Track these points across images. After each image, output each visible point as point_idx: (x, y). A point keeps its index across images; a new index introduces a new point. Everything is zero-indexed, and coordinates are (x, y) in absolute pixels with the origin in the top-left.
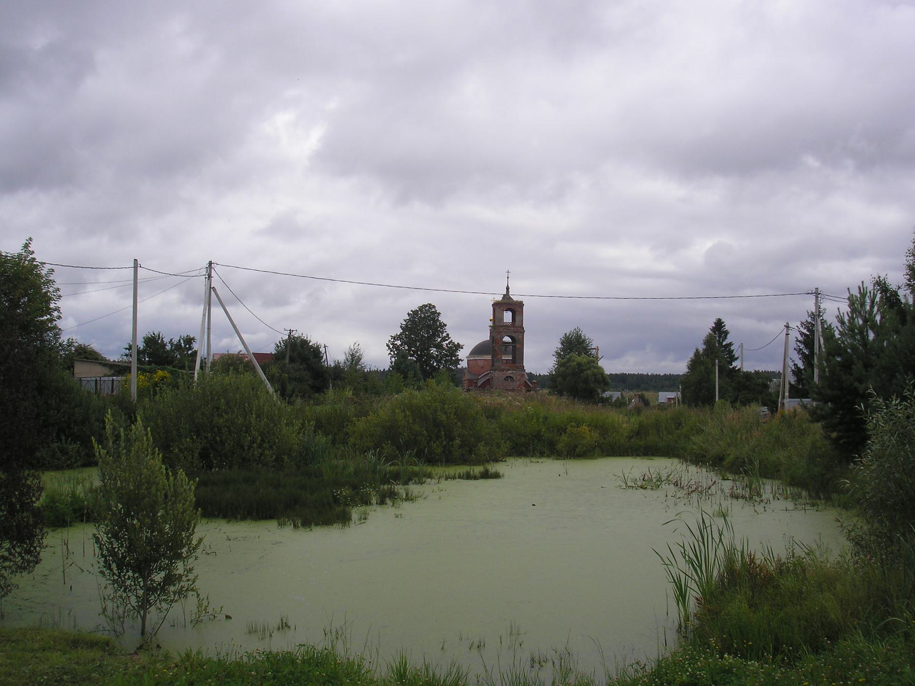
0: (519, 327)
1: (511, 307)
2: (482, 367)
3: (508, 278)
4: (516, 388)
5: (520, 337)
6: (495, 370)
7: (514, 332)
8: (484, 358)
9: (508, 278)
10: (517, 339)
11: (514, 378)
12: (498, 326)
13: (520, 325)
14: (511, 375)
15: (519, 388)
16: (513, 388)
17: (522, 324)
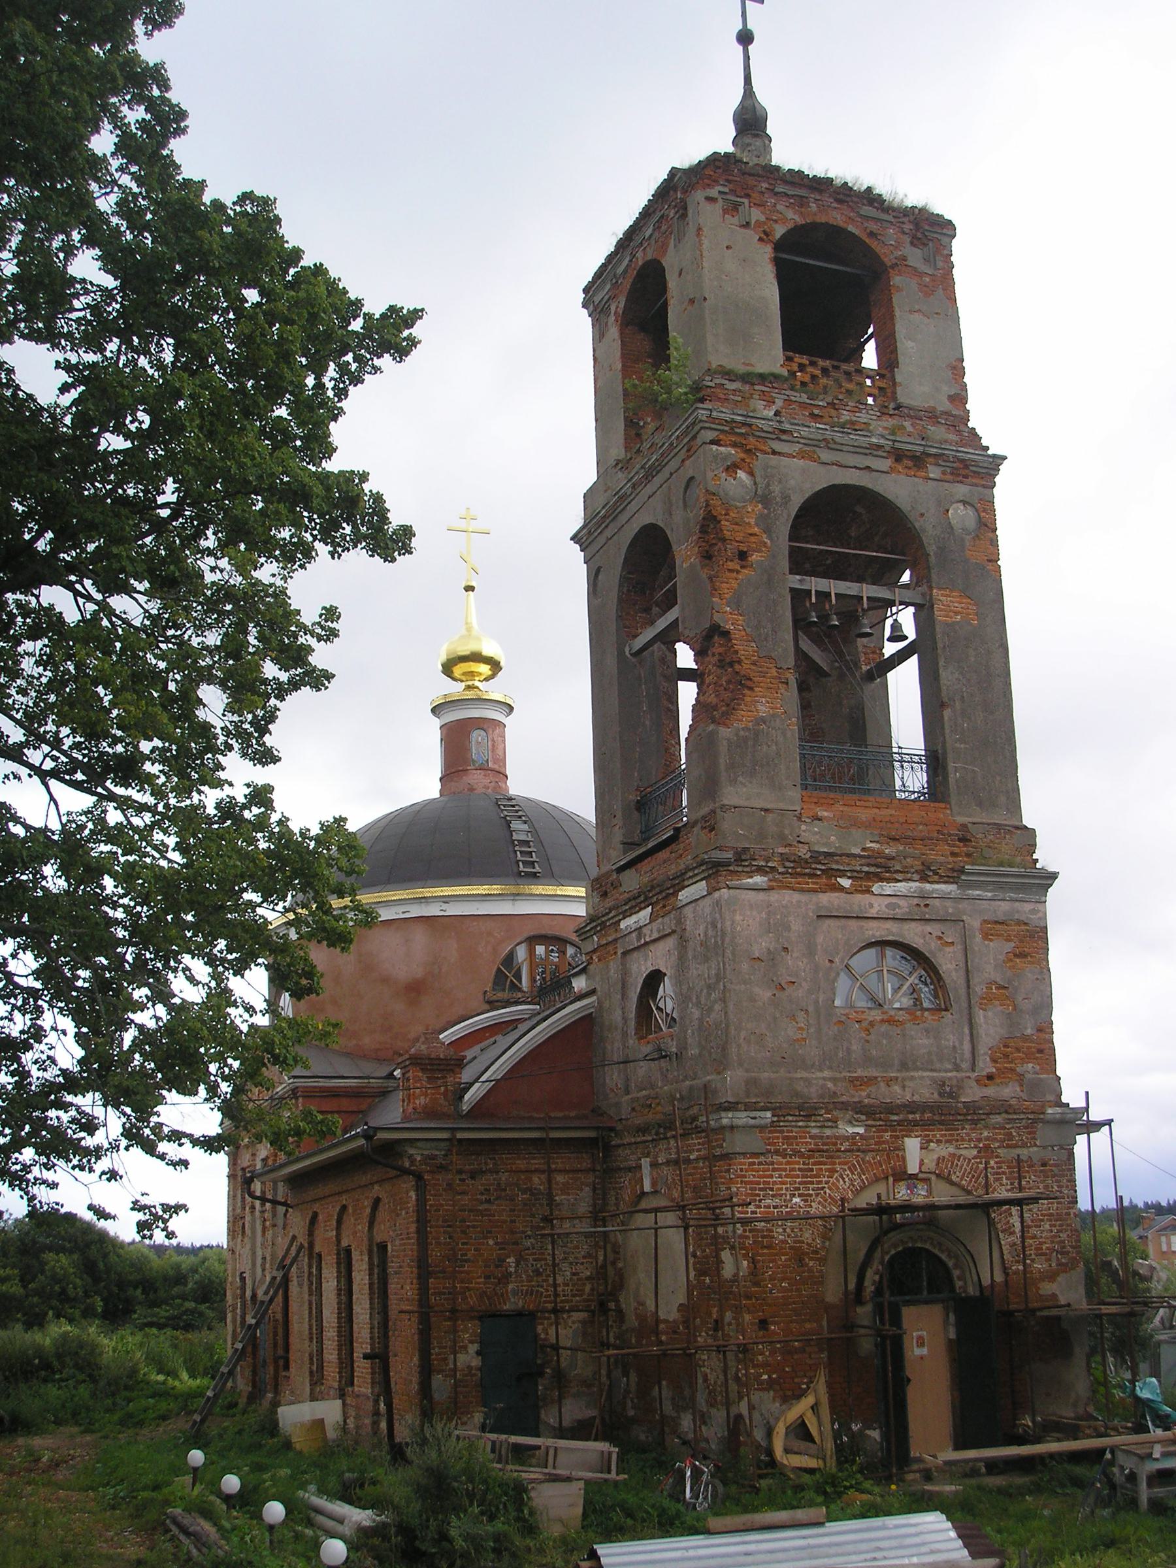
0: (933, 416)
1: (837, 217)
2: (415, 990)
3: (745, 38)
4: (973, 1093)
5: (960, 515)
6: (743, 861)
7: (898, 456)
8: (433, 910)
9: (745, 38)
10: (928, 527)
11: (948, 963)
12: (729, 375)
13: (944, 405)
14: (913, 934)
15: (1008, 1091)
16: (948, 1091)
17: (960, 398)
